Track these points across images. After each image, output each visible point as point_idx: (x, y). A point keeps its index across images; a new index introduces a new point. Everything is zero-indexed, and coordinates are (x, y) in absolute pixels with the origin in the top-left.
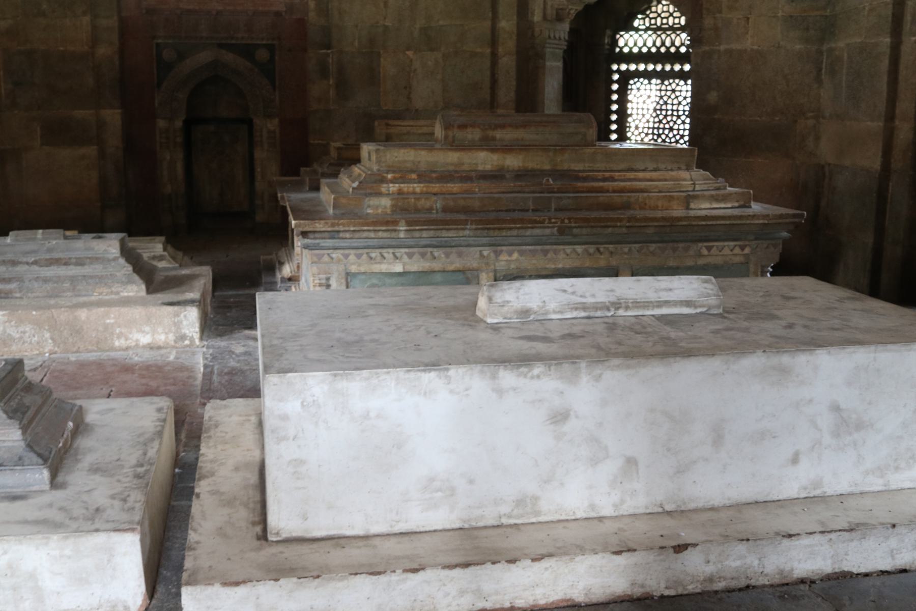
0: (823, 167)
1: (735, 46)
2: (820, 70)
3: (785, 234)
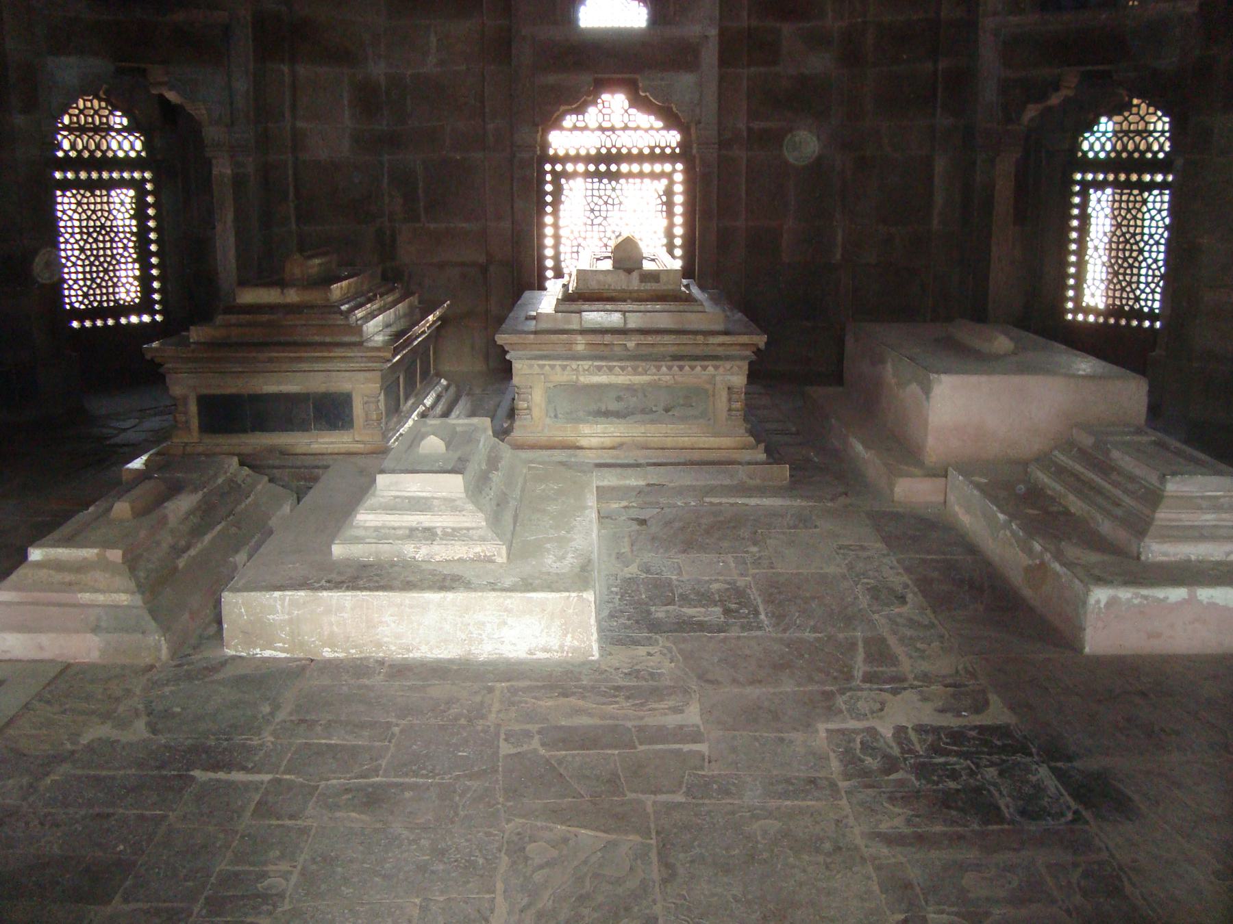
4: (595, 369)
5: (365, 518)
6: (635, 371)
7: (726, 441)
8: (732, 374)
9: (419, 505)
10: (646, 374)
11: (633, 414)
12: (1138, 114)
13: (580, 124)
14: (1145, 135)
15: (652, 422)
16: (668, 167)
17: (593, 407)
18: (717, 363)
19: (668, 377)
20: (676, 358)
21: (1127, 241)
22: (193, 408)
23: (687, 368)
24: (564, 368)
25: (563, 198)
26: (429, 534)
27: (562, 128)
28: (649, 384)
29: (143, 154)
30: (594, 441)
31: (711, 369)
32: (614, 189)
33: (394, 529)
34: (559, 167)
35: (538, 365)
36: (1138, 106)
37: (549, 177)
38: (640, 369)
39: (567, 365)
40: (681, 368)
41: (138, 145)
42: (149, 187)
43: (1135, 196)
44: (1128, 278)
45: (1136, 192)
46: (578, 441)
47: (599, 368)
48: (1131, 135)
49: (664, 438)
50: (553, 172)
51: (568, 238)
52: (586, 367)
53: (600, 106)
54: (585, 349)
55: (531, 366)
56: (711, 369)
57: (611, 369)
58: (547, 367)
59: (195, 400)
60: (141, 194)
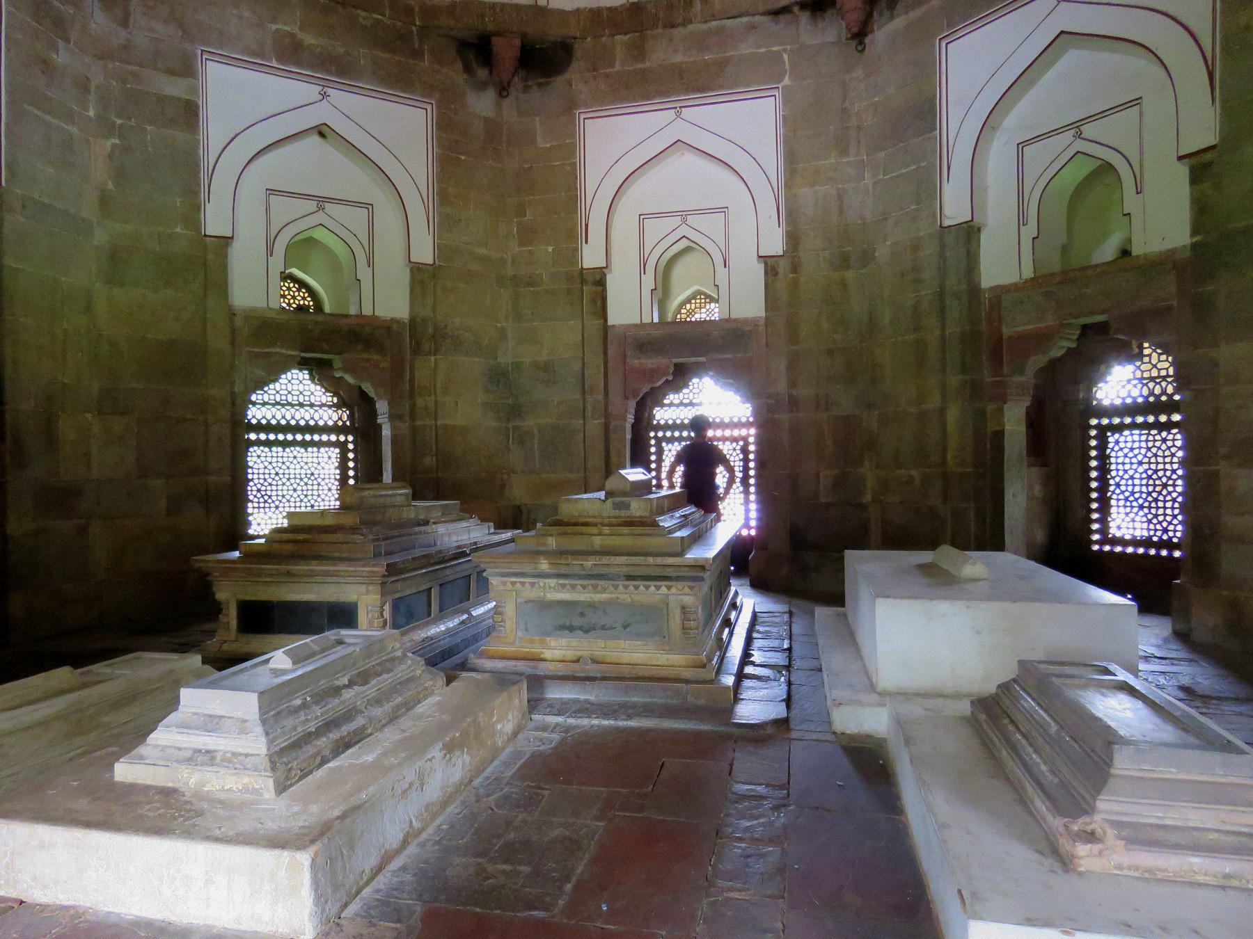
0: (519, 507)
1: (447, 422)
4: (560, 588)
5: (162, 736)
7: (677, 659)
9: (212, 724)
10: (605, 593)
11: (594, 629)
12: (1150, 362)
14: (1158, 381)
15: (612, 638)
16: (744, 432)
19: (625, 596)
20: (630, 578)
21: (1149, 477)
24: (533, 584)
25: (664, 457)
26: (208, 757)
27: (663, 405)
28: (610, 602)
29: (348, 423)
30: (558, 654)
31: (664, 590)
33: (180, 749)
34: (660, 434)
36: (1149, 356)
37: (653, 442)
38: (599, 588)
39: (535, 583)
40: (636, 587)
41: (345, 418)
42: (351, 446)
43: (1154, 436)
44: (1153, 511)
45: (1154, 432)
46: (542, 653)
47: (563, 586)
48: (1145, 382)
49: (619, 654)
50: (656, 437)
52: (552, 585)
53: (691, 387)
54: (549, 569)
55: (504, 583)
56: (664, 590)
57: (573, 587)
58: (518, 585)
59: (235, 606)
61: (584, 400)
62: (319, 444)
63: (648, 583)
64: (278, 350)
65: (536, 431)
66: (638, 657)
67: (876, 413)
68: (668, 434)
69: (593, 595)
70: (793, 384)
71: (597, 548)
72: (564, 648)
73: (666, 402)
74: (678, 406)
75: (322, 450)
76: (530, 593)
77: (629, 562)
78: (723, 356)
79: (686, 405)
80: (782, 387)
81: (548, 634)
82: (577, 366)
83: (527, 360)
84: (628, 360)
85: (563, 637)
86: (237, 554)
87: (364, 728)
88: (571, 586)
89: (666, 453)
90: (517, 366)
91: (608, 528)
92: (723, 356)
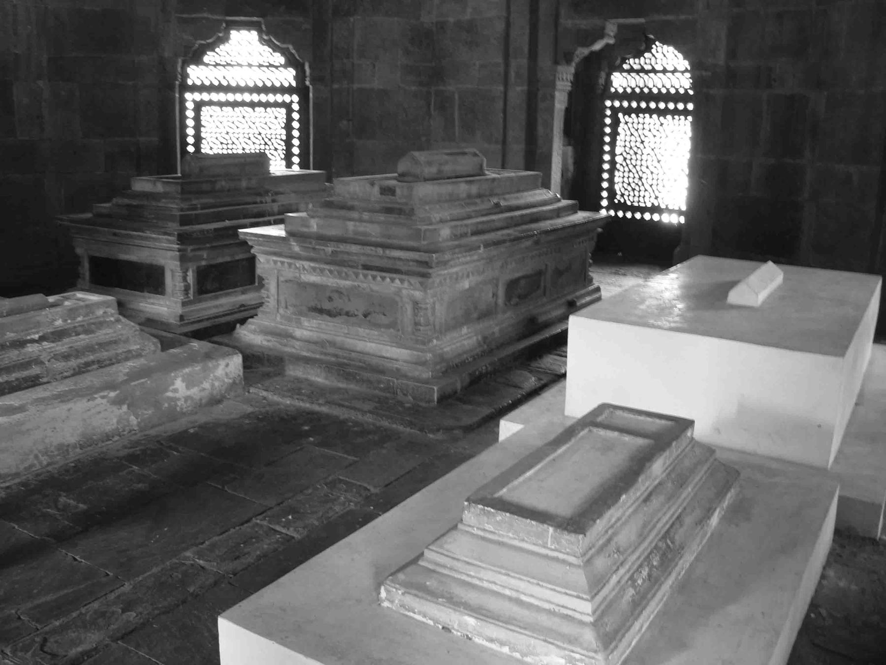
1: (364, 86)
2: (429, 105)
3: (600, 230)
4: (312, 270)
6: (340, 275)
8: (415, 289)
11: (340, 315)
13: (636, 67)
17: (312, 304)
18: (403, 277)
19: (365, 285)
20: (366, 267)
22: (86, 265)
23: (379, 278)
25: (620, 130)
27: (622, 70)
32: (662, 125)
34: (617, 104)
35: (273, 260)
37: (608, 112)
40: (374, 278)
42: (296, 107)
47: (314, 269)
50: (612, 108)
51: (621, 165)
58: (279, 264)
60: (290, 111)
61: (507, 65)
62: (267, 105)
63: (384, 274)
64: (205, 15)
65: (457, 96)
66: (370, 347)
67: (826, 93)
68: (625, 104)
69: (339, 281)
70: (732, 54)
71: (350, 235)
72: (314, 329)
73: (626, 67)
74: (638, 72)
75: (268, 109)
76: (288, 274)
77: (362, 251)
78: (664, 18)
79: (647, 72)
80: (721, 58)
81: (301, 313)
82: (500, 26)
83: (451, 20)
84: (562, 21)
85: (314, 318)
86: (89, 215)
87: (37, 377)
88: (320, 270)
89: (622, 125)
90: (442, 26)
91: (366, 213)
92: (664, 18)
